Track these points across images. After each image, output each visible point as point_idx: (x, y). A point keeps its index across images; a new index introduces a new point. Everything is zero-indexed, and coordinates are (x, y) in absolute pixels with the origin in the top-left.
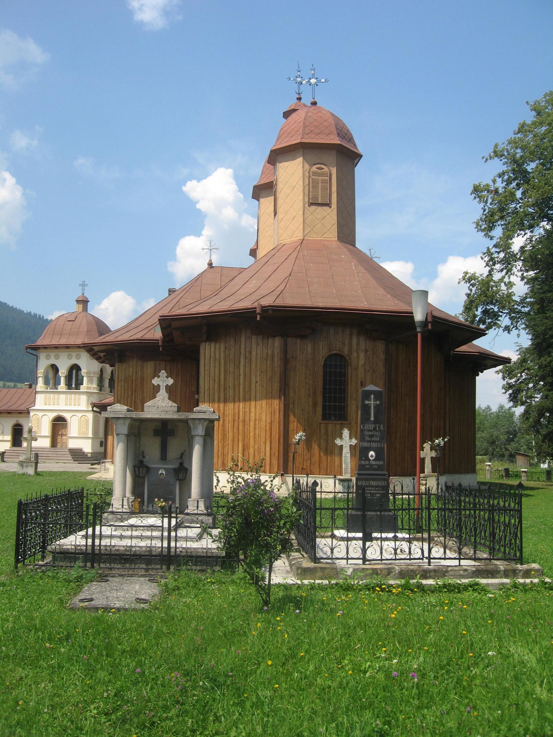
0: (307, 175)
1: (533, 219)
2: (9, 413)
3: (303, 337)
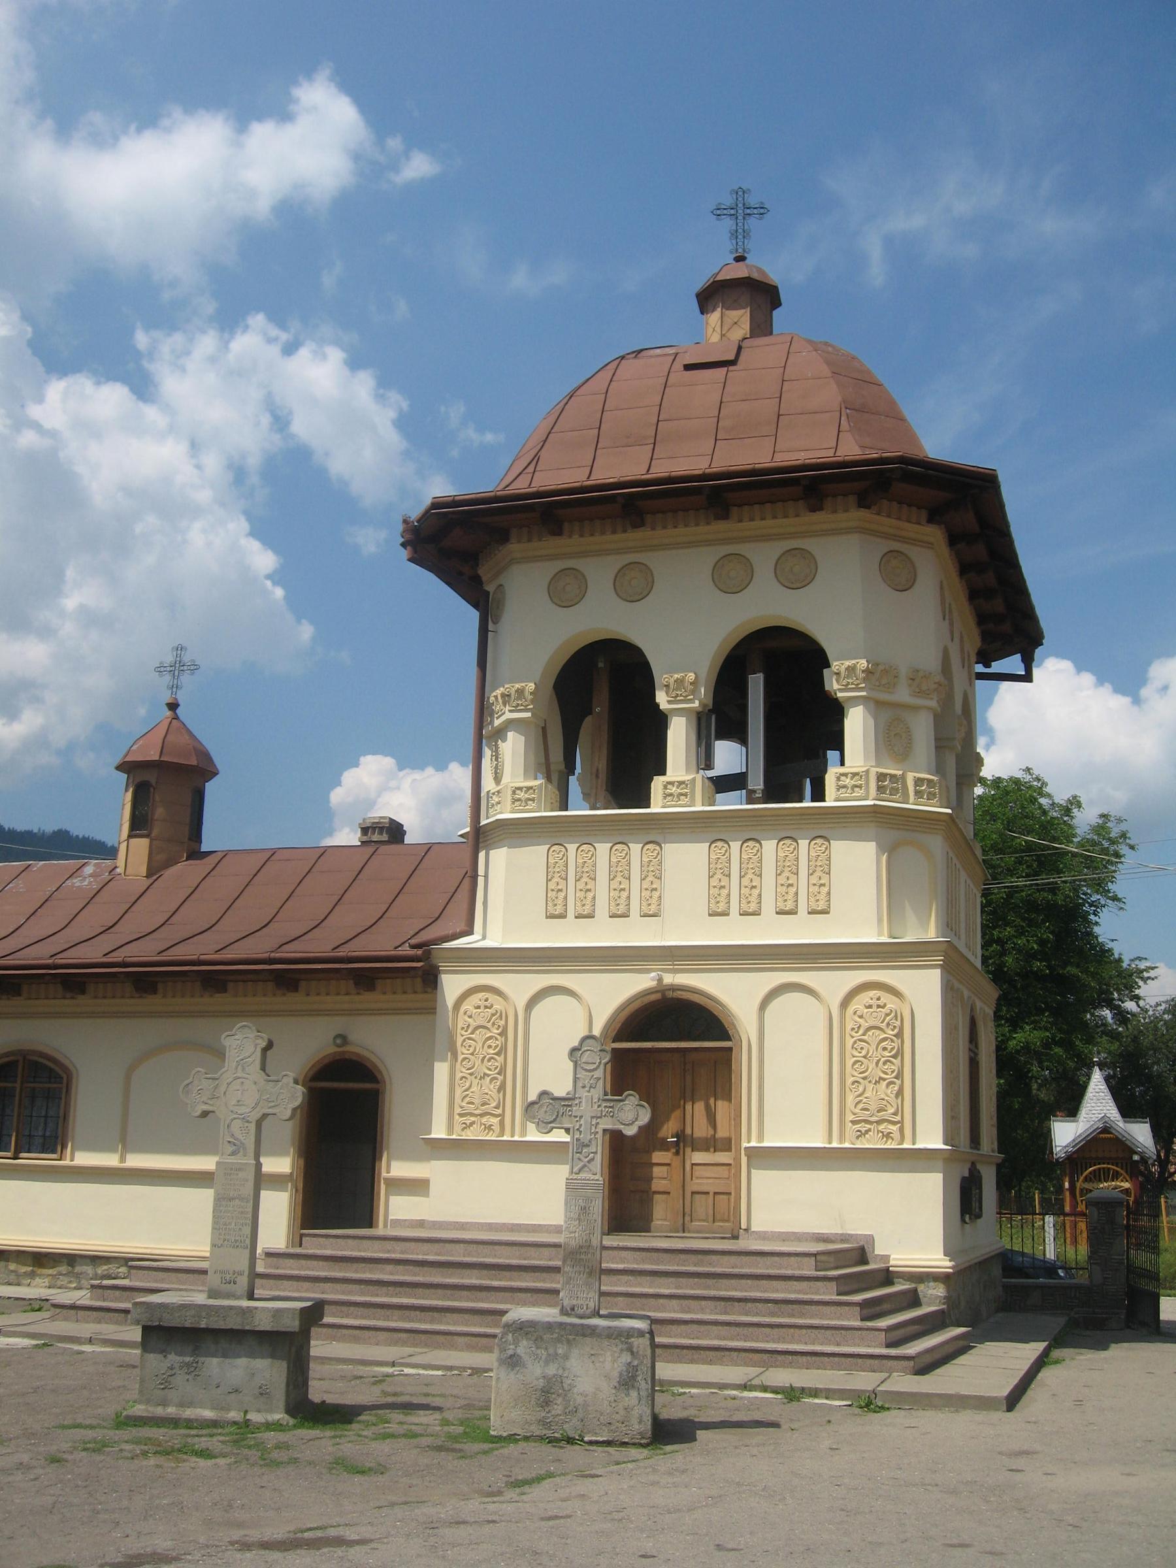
2: (284, 980)
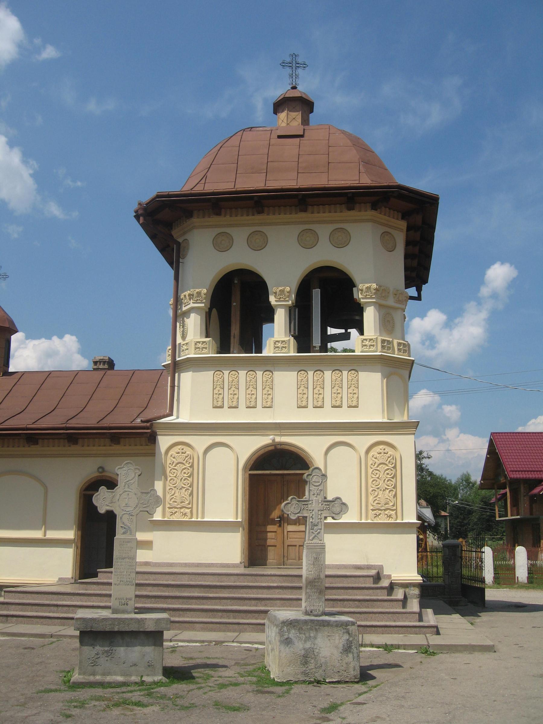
2: (71, 438)
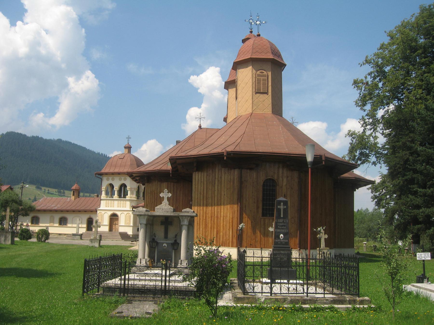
0: (255, 76)
1: (389, 99)
2: (85, 211)
3: (251, 169)
